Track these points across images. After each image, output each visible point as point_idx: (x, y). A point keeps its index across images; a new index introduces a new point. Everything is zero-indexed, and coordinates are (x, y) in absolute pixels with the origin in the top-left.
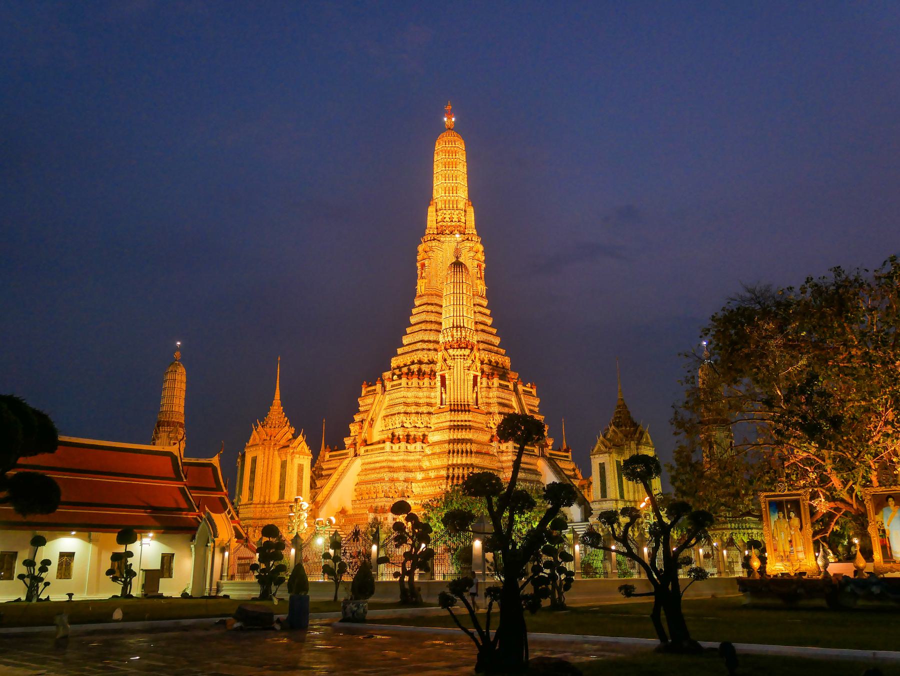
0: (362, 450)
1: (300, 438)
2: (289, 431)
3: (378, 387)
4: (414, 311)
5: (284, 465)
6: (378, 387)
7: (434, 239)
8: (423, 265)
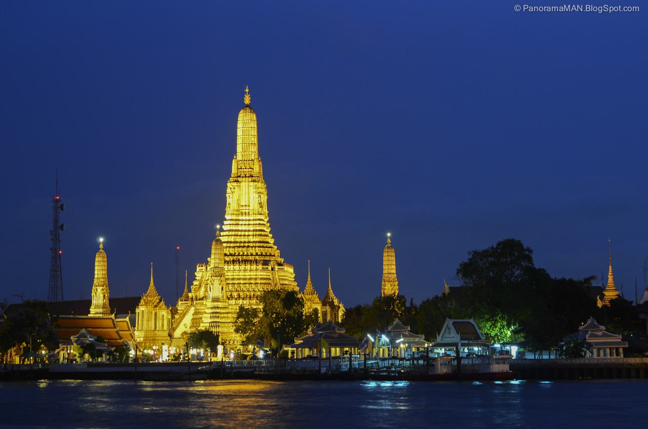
0: (195, 302)
1: (162, 302)
2: (156, 299)
3: (204, 268)
4: (225, 222)
5: (156, 314)
6: (204, 268)
7: (236, 181)
8: (229, 196)
